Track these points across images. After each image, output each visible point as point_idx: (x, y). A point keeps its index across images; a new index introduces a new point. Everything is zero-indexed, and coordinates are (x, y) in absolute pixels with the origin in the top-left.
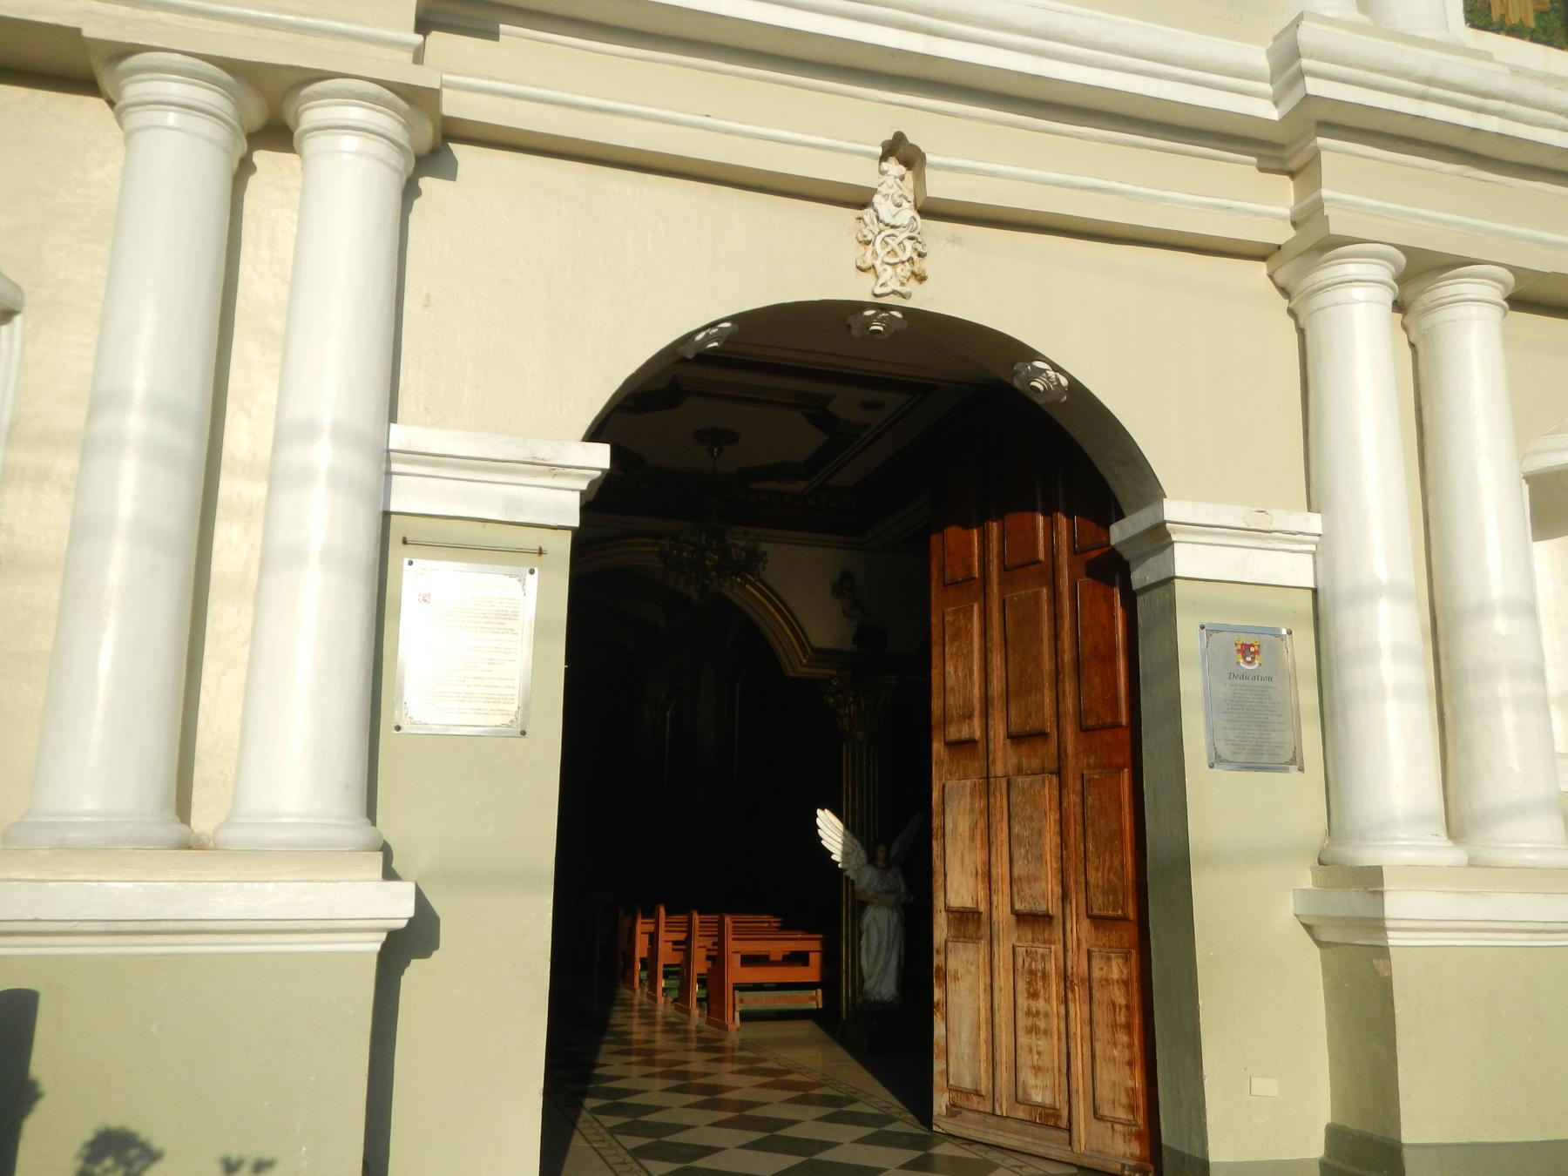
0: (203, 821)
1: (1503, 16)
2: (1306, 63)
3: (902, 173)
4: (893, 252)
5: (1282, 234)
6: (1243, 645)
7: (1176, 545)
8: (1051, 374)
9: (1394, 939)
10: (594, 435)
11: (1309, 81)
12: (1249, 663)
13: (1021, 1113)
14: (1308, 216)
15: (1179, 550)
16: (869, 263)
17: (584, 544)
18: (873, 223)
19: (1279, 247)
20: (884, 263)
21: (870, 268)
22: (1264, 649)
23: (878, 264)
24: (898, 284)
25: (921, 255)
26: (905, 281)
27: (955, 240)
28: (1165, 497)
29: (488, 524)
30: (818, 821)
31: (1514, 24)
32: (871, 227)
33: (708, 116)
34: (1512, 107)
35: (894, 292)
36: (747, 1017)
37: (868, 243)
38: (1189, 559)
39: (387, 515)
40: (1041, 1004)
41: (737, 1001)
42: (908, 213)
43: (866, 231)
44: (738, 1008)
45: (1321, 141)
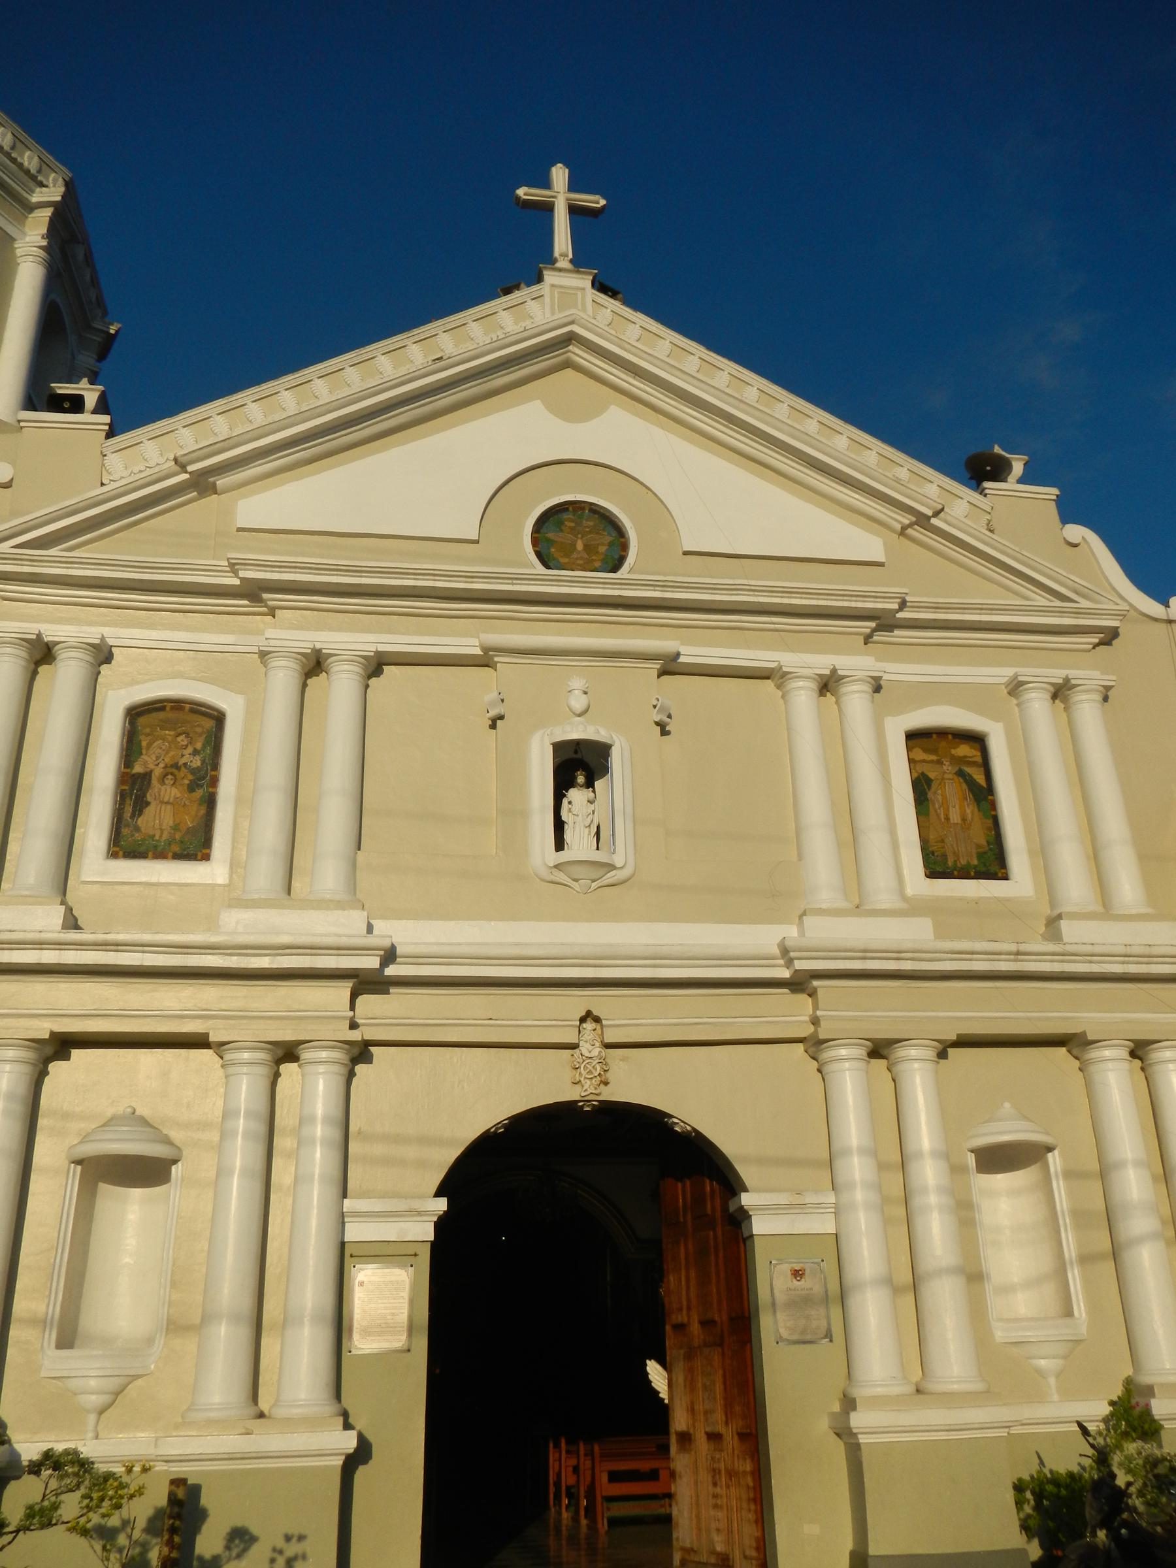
0: (264, 1405)
1: (955, 861)
2: (792, 954)
3: (594, 1028)
4: (590, 1072)
5: (807, 1031)
6: (796, 1270)
7: (753, 1217)
8: (682, 1124)
9: (862, 1439)
10: (438, 1194)
11: (796, 962)
12: (799, 1280)
13: (713, 1560)
14: (815, 1021)
15: (754, 1219)
16: (578, 1080)
17: (437, 1248)
18: (579, 1058)
19: (805, 1038)
20: (585, 1078)
21: (578, 1082)
22: (807, 1272)
23: (582, 1079)
24: (593, 1089)
25: (605, 1071)
26: (597, 1087)
27: (624, 1059)
28: (746, 1190)
29: (390, 1243)
30: (648, 1368)
31: (965, 865)
32: (578, 1060)
33: (491, 1019)
34: (916, 955)
35: (591, 1093)
36: (613, 1522)
37: (577, 1068)
38: (759, 1226)
39: (343, 1244)
40: (718, 1490)
41: (605, 1510)
42: (596, 1052)
43: (575, 1063)
44: (605, 1515)
45: (815, 983)
